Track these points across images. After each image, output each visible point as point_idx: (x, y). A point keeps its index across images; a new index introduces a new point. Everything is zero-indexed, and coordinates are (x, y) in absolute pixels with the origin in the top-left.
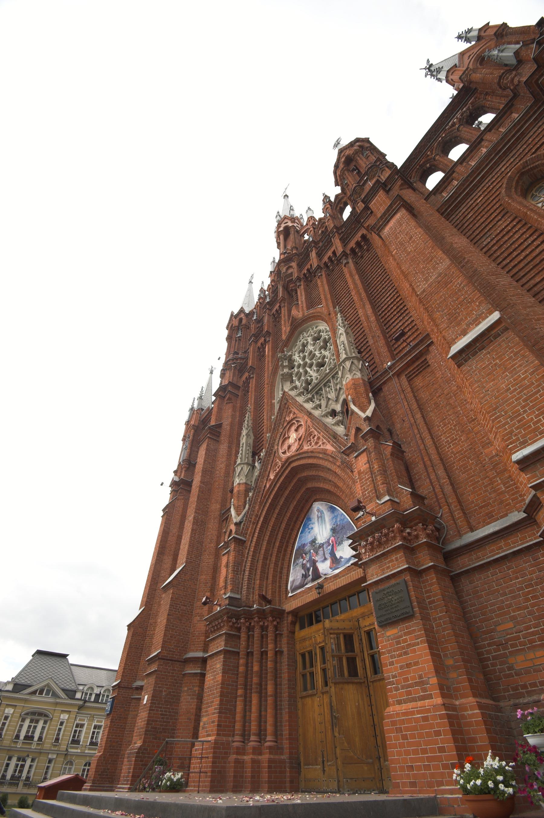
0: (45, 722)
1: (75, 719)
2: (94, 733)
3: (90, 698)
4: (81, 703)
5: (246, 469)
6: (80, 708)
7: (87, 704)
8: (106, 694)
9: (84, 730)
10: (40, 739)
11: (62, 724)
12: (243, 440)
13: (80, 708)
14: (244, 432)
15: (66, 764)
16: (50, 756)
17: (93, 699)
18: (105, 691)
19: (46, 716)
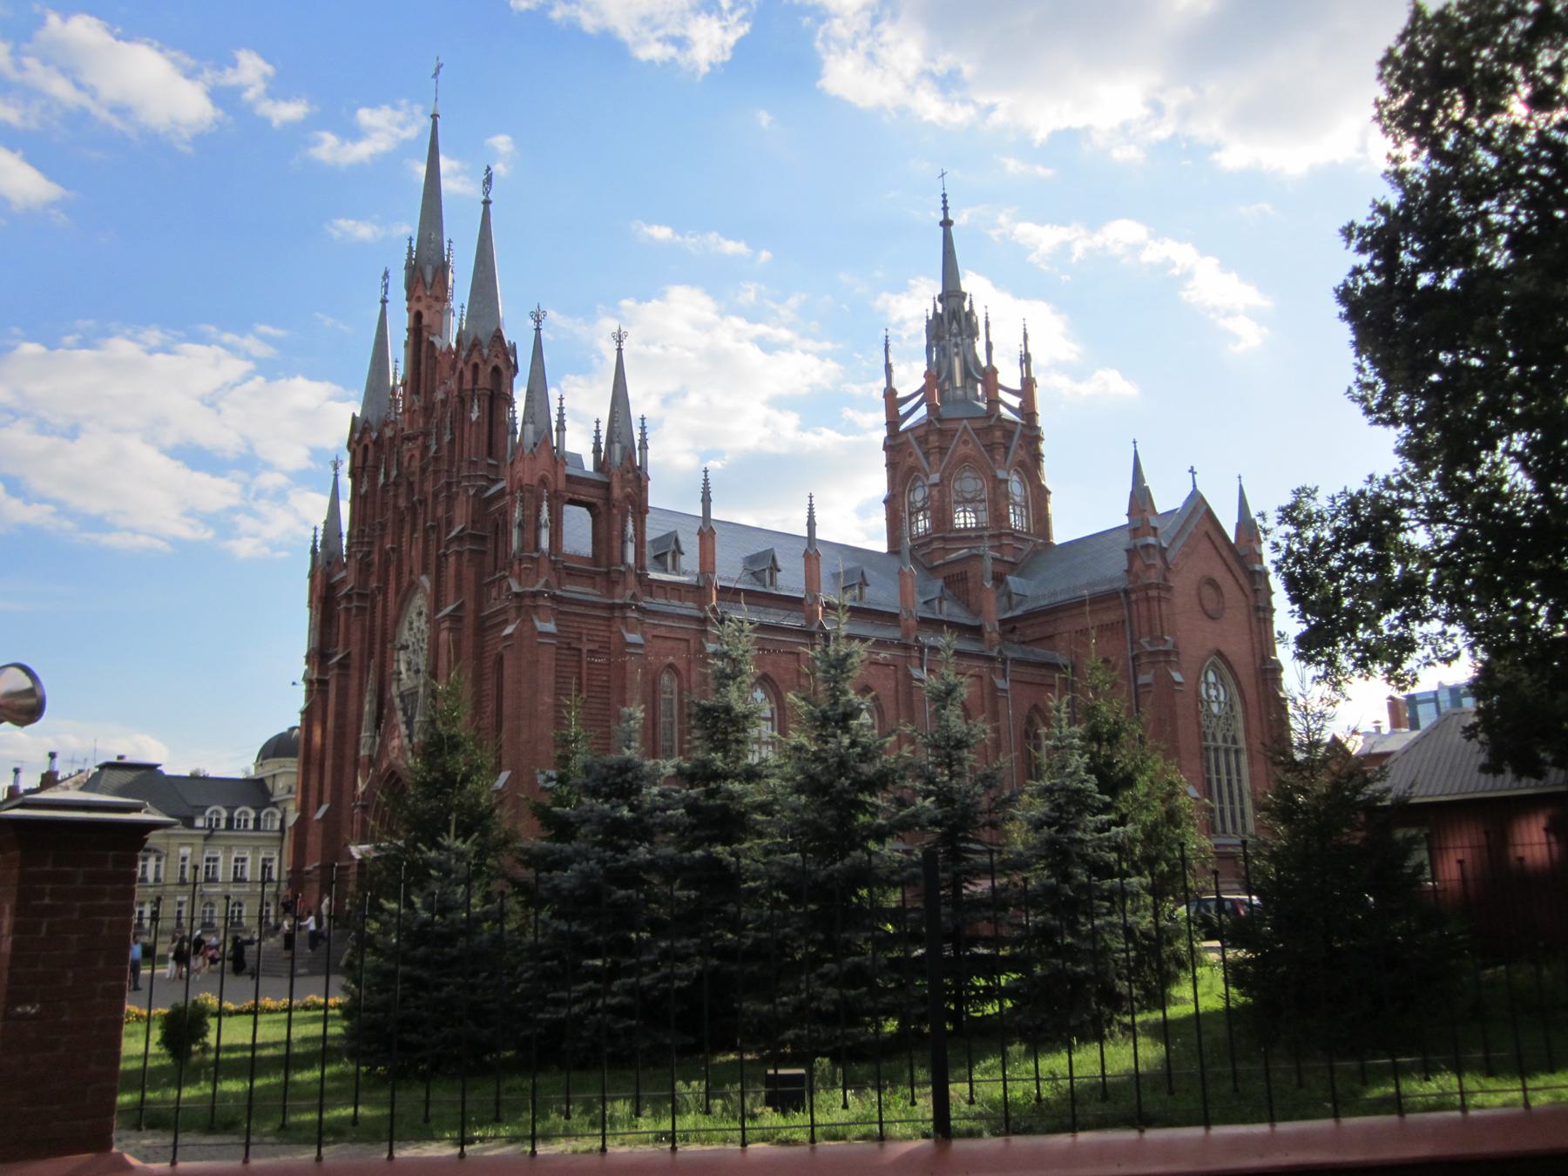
0: (158, 859)
1: (203, 852)
2: (236, 867)
3: (217, 825)
4: (207, 832)
5: (370, 741)
6: (207, 838)
7: (216, 833)
8: (243, 818)
9: (220, 864)
10: (157, 879)
11: (184, 859)
12: (367, 707)
13: (207, 838)
14: (367, 698)
15: (205, 905)
16: (179, 899)
17: (223, 824)
18: (240, 814)
19: (155, 851)
